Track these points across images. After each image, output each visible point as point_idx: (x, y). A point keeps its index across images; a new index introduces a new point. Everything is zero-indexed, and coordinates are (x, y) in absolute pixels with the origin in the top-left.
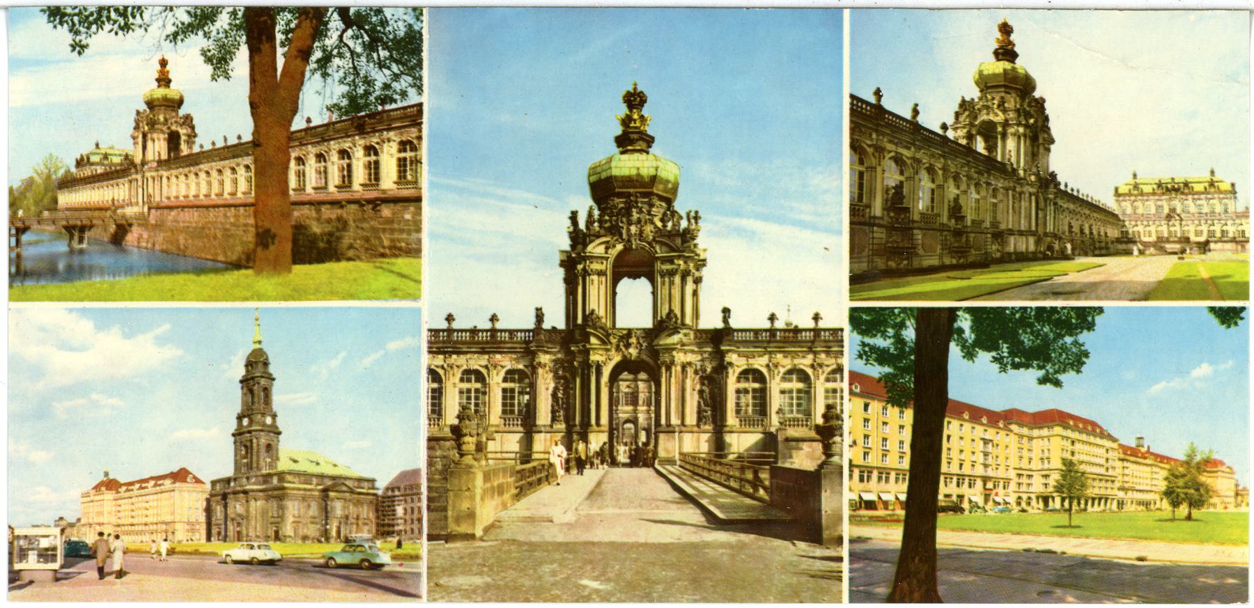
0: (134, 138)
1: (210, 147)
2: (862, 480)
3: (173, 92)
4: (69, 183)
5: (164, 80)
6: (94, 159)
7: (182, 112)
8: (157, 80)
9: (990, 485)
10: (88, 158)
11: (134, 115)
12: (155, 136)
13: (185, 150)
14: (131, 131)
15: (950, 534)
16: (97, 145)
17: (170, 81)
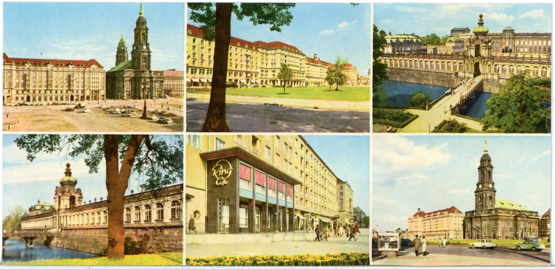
0: (55, 198)
1: (89, 203)
2: (192, 73)
3: (72, 178)
4: (26, 218)
5: (68, 173)
6: (38, 208)
7: (77, 187)
8: (66, 173)
9: (249, 75)
10: (35, 208)
11: (55, 189)
12: (64, 198)
13: (77, 204)
14: (54, 196)
15: (231, 96)
16: (39, 202)
17: (71, 173)
